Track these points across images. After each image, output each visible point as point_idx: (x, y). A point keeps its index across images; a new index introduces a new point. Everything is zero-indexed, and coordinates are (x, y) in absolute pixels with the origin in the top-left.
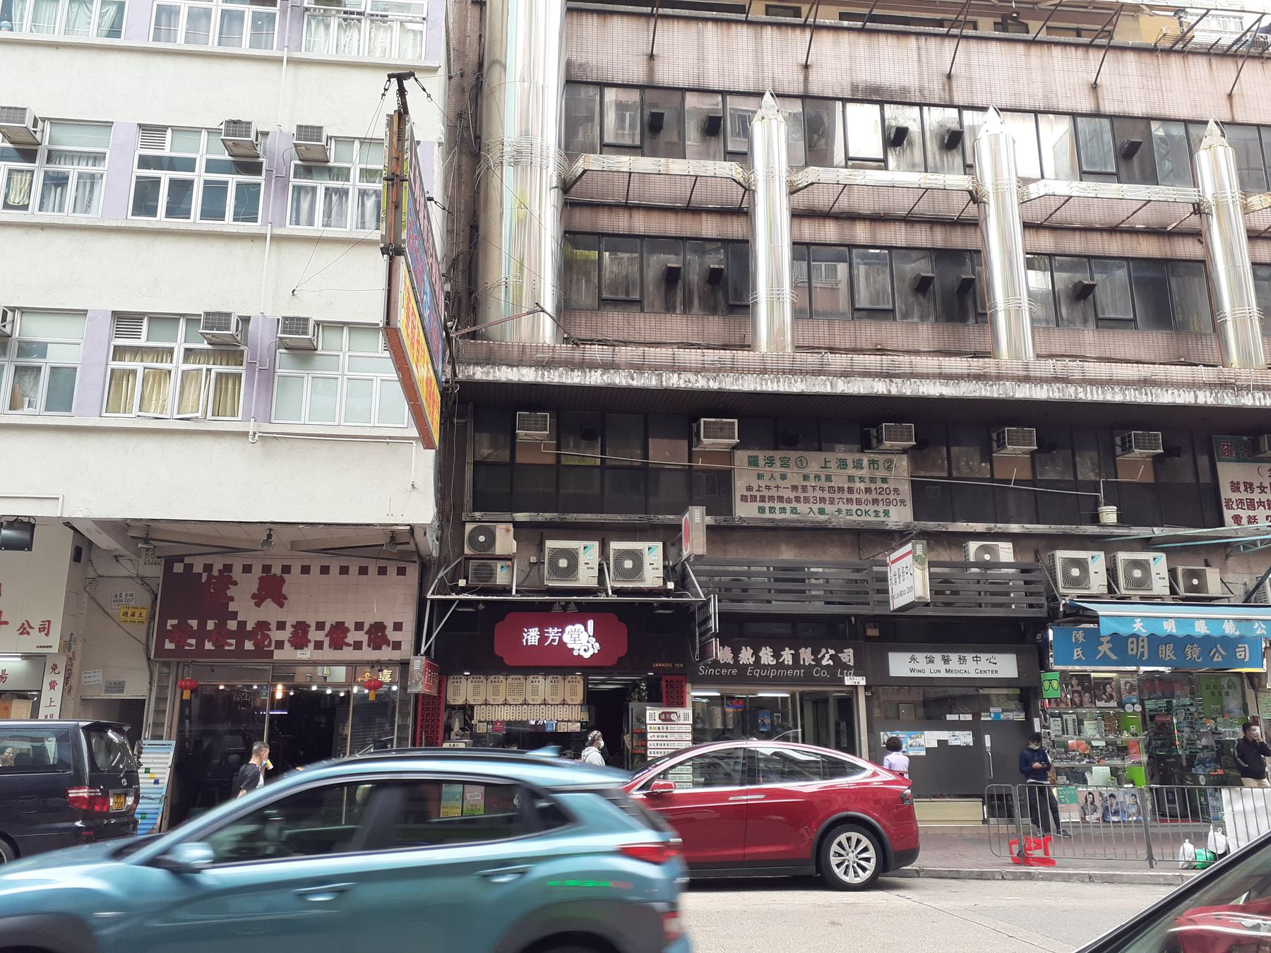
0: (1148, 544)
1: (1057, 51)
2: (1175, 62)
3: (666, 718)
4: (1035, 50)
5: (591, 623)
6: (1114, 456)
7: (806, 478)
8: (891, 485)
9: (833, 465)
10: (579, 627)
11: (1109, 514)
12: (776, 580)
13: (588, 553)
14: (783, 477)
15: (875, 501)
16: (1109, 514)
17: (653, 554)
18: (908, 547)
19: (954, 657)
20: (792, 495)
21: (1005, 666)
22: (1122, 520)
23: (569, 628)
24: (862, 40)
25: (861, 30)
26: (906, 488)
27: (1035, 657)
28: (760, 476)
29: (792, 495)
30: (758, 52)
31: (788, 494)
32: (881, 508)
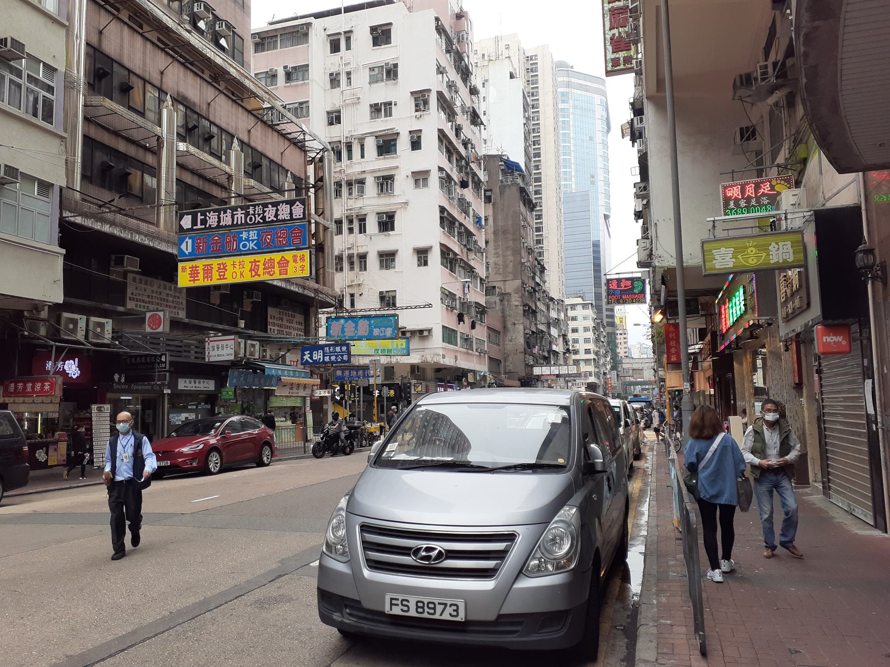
0: (250, 337)
1: (240, 109)
2: (270, 130)
3: (99, 410)
4: (234, 105)
5: (76, 360)
6: (243, 299)
7: (153, 292)
8: (180, 300)
9: (162, 287)
10: (72, 361)
11: (242, 324)
12: (151, 343)
13: (82, 320)
14: (145, 290)
15: (175, 307)
16: (242, 324)
17: (109, 324)
18: (232, 337)
19: (197, 381)
20: (147, 300)
21: (209, 385)
22: (246, 327)
23: (67, 362)
24: (182, 69)
25: (183, 64)
26: (184, 302)
27: (221, 383)
28: (137, 289)
29: (147, 300)
30: (144, 53)
31: (147, 299)
32: (176, 311)
